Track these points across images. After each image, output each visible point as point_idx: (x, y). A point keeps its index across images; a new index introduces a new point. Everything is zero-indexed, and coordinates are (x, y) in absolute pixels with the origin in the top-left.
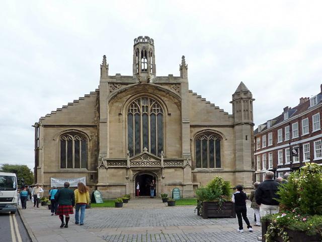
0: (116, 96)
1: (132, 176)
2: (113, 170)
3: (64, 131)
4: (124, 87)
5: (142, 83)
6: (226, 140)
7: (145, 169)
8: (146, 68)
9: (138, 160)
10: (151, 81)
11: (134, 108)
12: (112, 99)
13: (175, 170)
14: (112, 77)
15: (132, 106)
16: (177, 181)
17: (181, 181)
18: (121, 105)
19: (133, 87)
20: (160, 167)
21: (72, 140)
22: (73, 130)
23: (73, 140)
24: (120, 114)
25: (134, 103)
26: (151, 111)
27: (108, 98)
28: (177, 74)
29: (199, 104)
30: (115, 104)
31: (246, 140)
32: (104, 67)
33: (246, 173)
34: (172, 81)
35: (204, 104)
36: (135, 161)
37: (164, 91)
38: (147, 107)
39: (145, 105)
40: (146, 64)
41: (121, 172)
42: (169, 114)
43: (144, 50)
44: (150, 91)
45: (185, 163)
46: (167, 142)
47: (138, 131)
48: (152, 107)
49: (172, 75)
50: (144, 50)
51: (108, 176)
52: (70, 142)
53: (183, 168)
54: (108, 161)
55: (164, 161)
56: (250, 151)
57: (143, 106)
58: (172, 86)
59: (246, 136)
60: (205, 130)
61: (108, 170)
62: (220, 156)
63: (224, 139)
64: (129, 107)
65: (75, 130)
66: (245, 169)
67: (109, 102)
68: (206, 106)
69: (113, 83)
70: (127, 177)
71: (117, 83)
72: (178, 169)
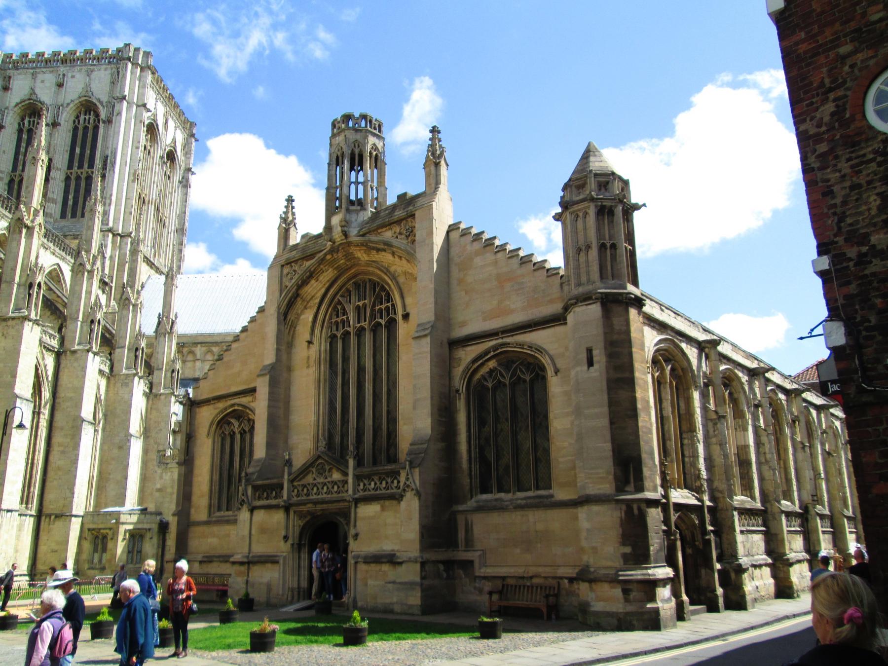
0: (296, 295)
1: (297, 530)
2: (263, 511)
3: (222, 412)
4: (308, 264)
5: (337, 244)
6: (557, 371)
7: (319, 507)
8: (361, 195)
9: (309, 479)
10: (353, 232)
11: (339, 320)
12: (290, 304)
13: (383, 509)
14: (296, 246)
15: (337, 317)
16: (387, 547)
17: (396, 548)
18: (311, 319)
19: (323, 260)
20: (345, 501)
21: (234, 433)
22: (233, 405)
23: (236, 431)
24: (310, 342)
25: (339, 303)
26: (373, 316)
27: (279, 308)
28: (415, 186)
29: (478, 261)
30: (302, 317)
31: (590, 363)
32: (287, 224)
33: (595, 508)
34: (399, 214)
35: (490, 257)
36: (300, 483)
37: (385, 250)
38: (365, 306)
39: (361, 304)
40: (361, 187)
41: (278, 517)
42: (406, 316)
43: (339, 154)
44: (361, 255)
45: (402, 479)
46: (400, 407)
47: (345, 384)
48: (374, 305)
49: (405, 194)
50: (339, 154)
51: (253, 532)
52: (232, 436)
53: (397, 498)
54: (256, 488)
55: (358, 478)
56: (606, 409)
57: (358, 307)
58: (397, 229)
59: (590, 351)
60: (495, 348)
61: (256, 513)
62: (612, 403)
63: (550, 372)
64: (331, 318)
65: (239, 405)
66: (593, 489)
67: (286, 315)
68: (496, 263)
69: (289, 263)
70: (283, 533)
71: (296, 262)
72: (387, 503)
